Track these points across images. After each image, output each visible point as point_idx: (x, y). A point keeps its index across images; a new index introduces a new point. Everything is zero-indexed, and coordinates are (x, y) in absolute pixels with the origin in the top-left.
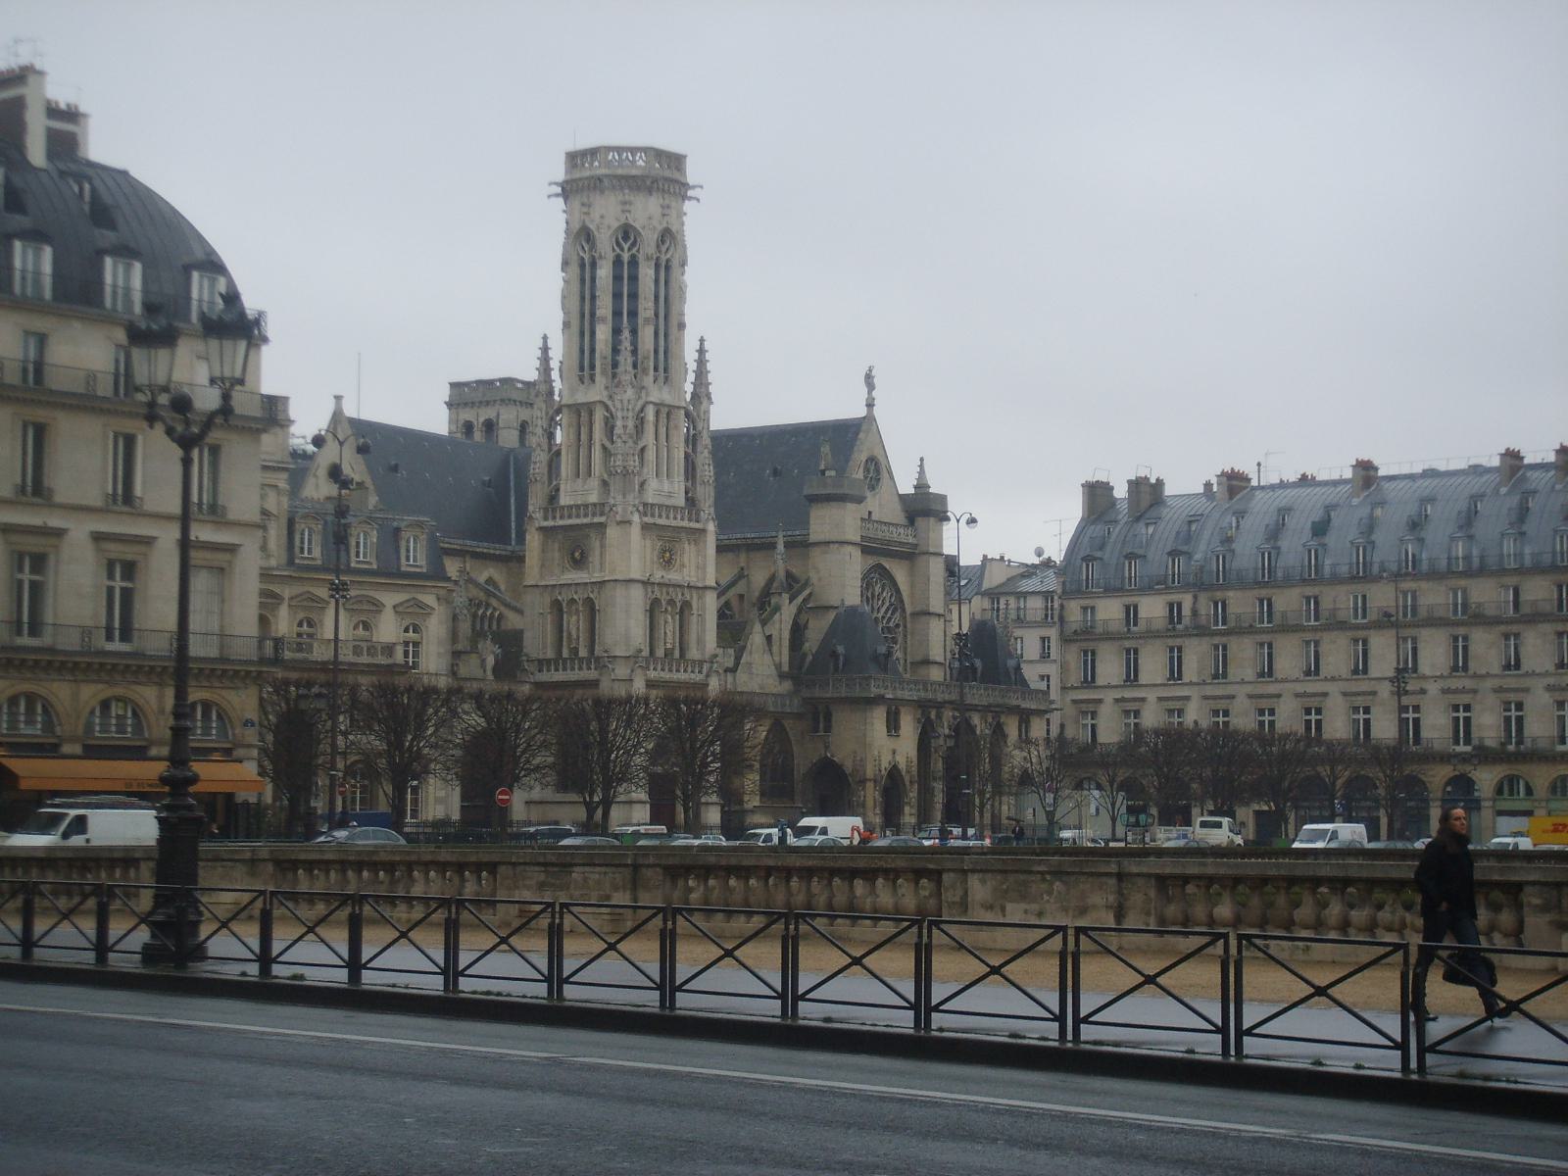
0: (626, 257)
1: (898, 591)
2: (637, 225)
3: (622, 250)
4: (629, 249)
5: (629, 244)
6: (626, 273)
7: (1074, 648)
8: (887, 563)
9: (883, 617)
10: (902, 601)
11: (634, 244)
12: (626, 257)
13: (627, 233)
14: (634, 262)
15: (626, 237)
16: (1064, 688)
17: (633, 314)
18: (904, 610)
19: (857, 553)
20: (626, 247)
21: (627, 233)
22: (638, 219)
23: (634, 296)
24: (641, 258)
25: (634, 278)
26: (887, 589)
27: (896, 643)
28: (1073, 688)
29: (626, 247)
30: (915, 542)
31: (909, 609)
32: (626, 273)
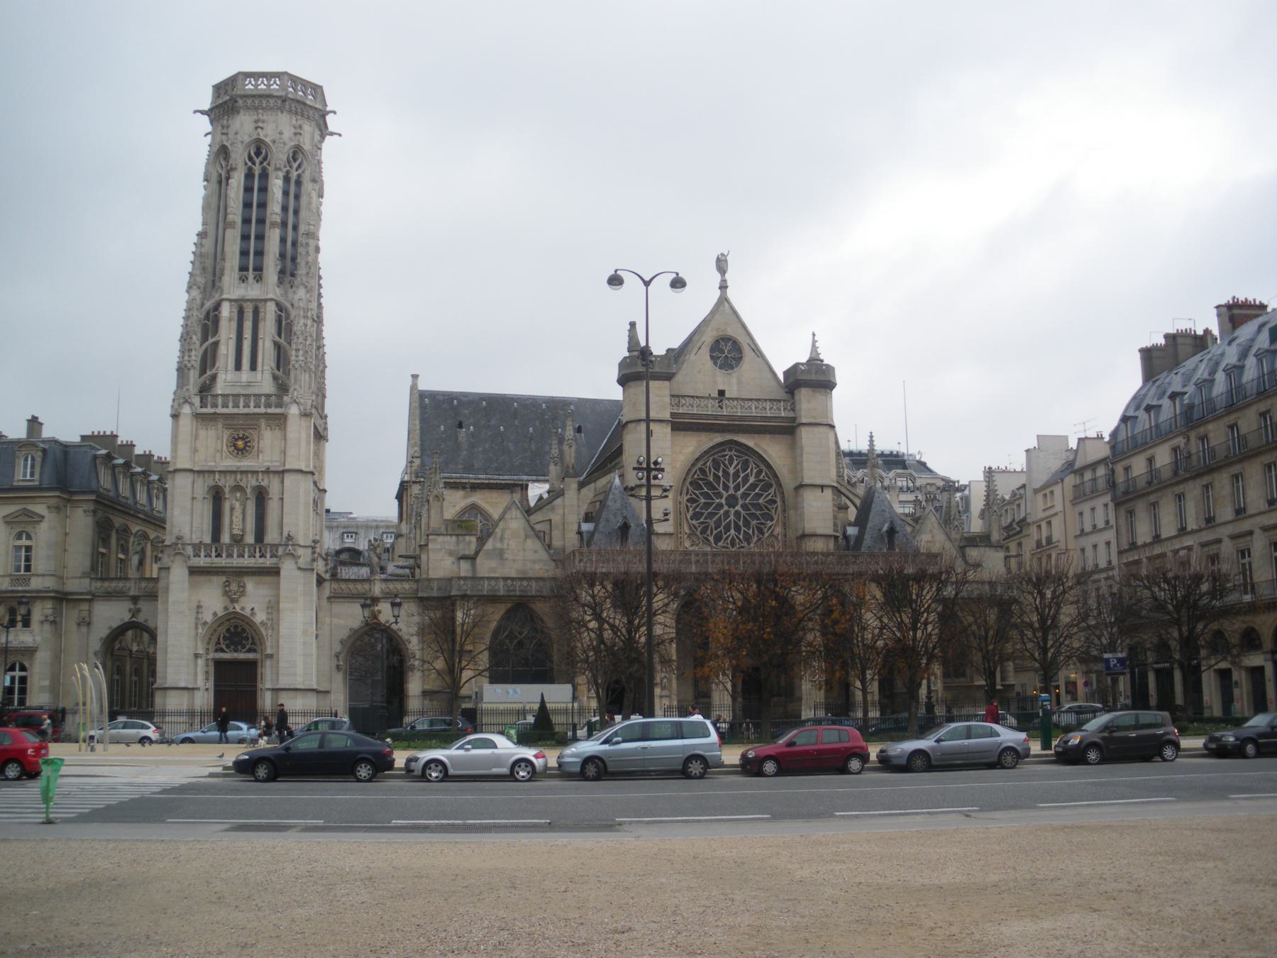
0: (257, 170)
1: (769, 466)
2: (267, 140)
3: (254, 163)
4: (261, 163)
5: (260, 158)
6: (256, 185)
7: (1122, 511)
8: (749, 441)
9: (745, 495)
10: (775, 476)
11: (265, 159)
12: (257, 170)
13: (259, 149)
14: (264, 175)
15: (258, 153)
16: (1120, 553)
17: (261, 221)
18: (780, 485)
19: (667, 429)
20: (258, 161)
21: (259, 149)
22: (268, 134)
23: (263, 205)
24: (270, 169)
25: (264, 189)
26: (752, 465)
27: (772, 519)
28: (1126, 551)
29: (258, 161)
30: (791, 414)
31: (788, 482)
32: (256, 185)
